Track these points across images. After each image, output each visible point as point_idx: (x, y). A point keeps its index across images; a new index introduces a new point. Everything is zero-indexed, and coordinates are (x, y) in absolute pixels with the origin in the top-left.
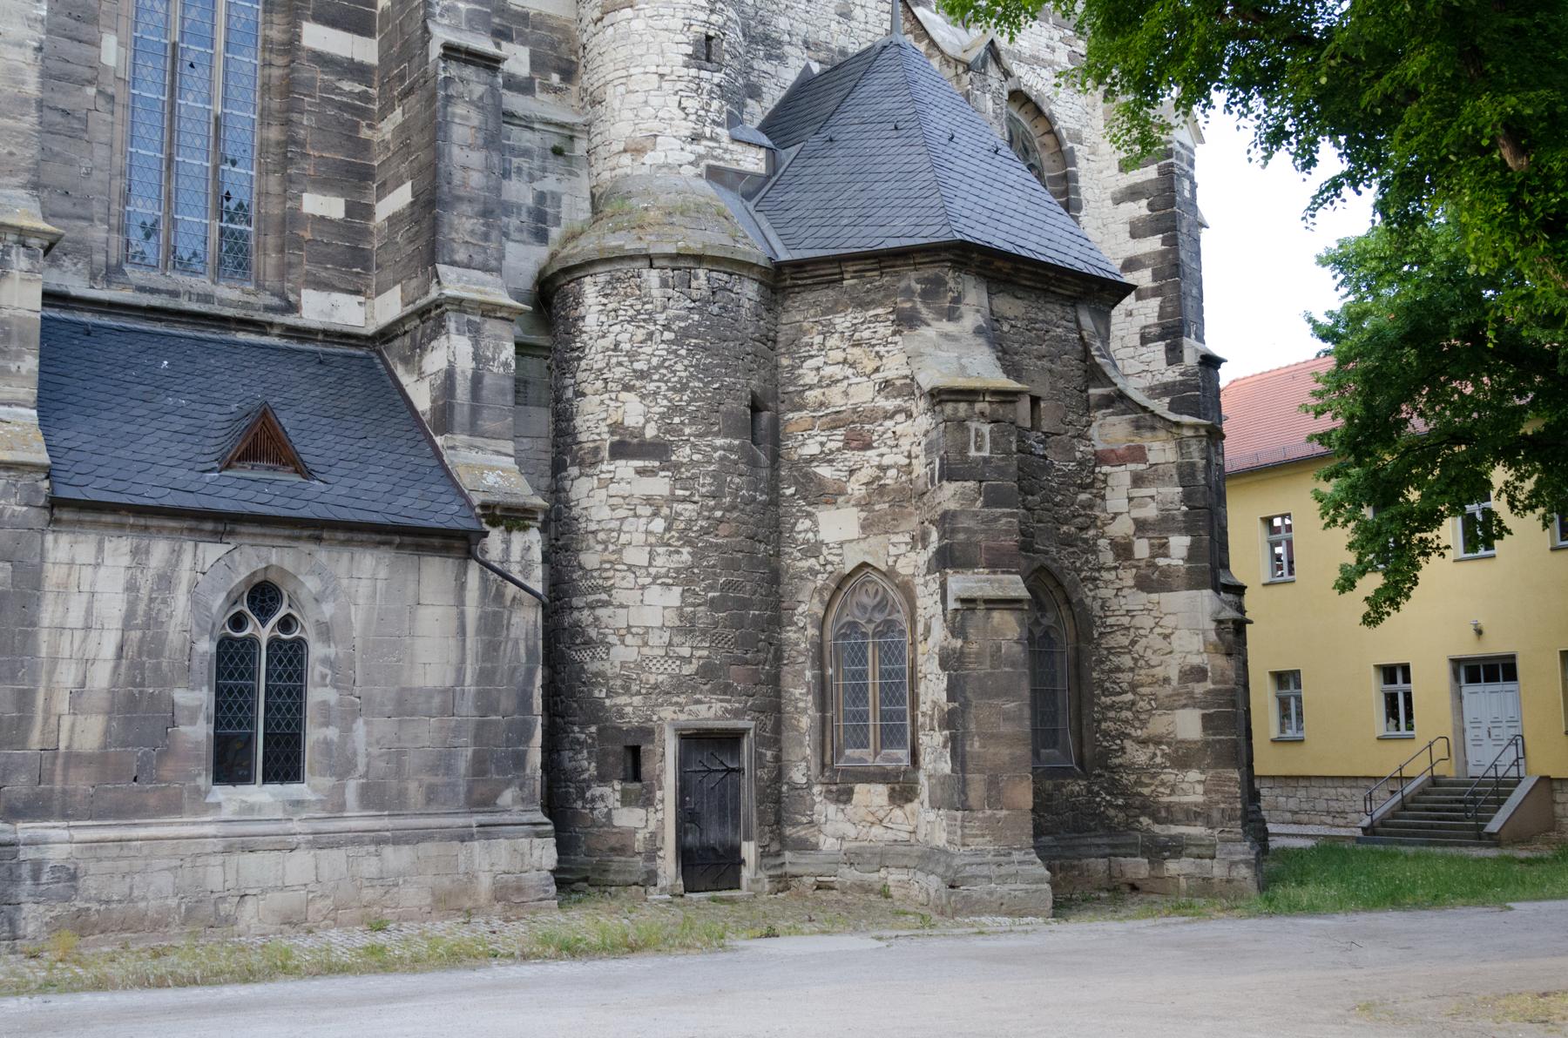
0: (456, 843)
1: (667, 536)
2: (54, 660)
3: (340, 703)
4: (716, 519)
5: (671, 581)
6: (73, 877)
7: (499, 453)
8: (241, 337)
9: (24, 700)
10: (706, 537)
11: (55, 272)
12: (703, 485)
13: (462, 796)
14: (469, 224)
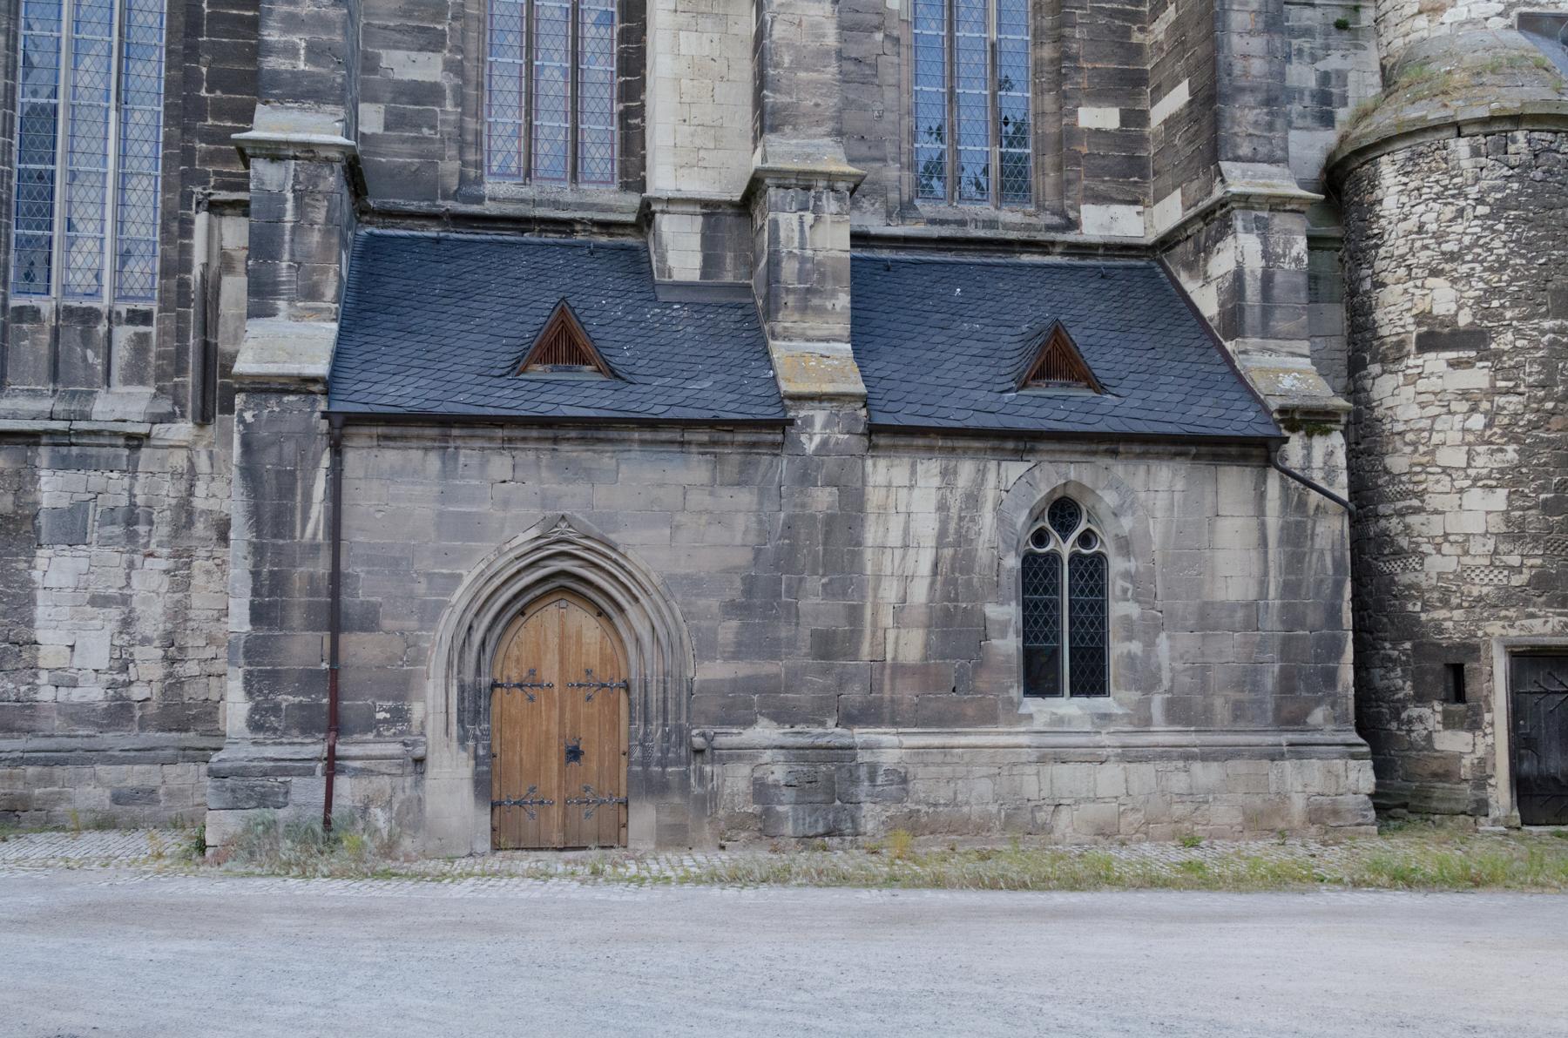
0: (1266, 763)
1: (1488, 433)
2: (878, 577)
3: (1143, 617)
4: (1546, 411)
5: (1494, 483)
6: (904, 780)
7: (1293, 354)
8: (1026, 258)
9: (855, 614)
10: (1535, 433)
11: (856, 213)
12: (1530, 374)
13: (1270, 714)
14: (1251, 115)
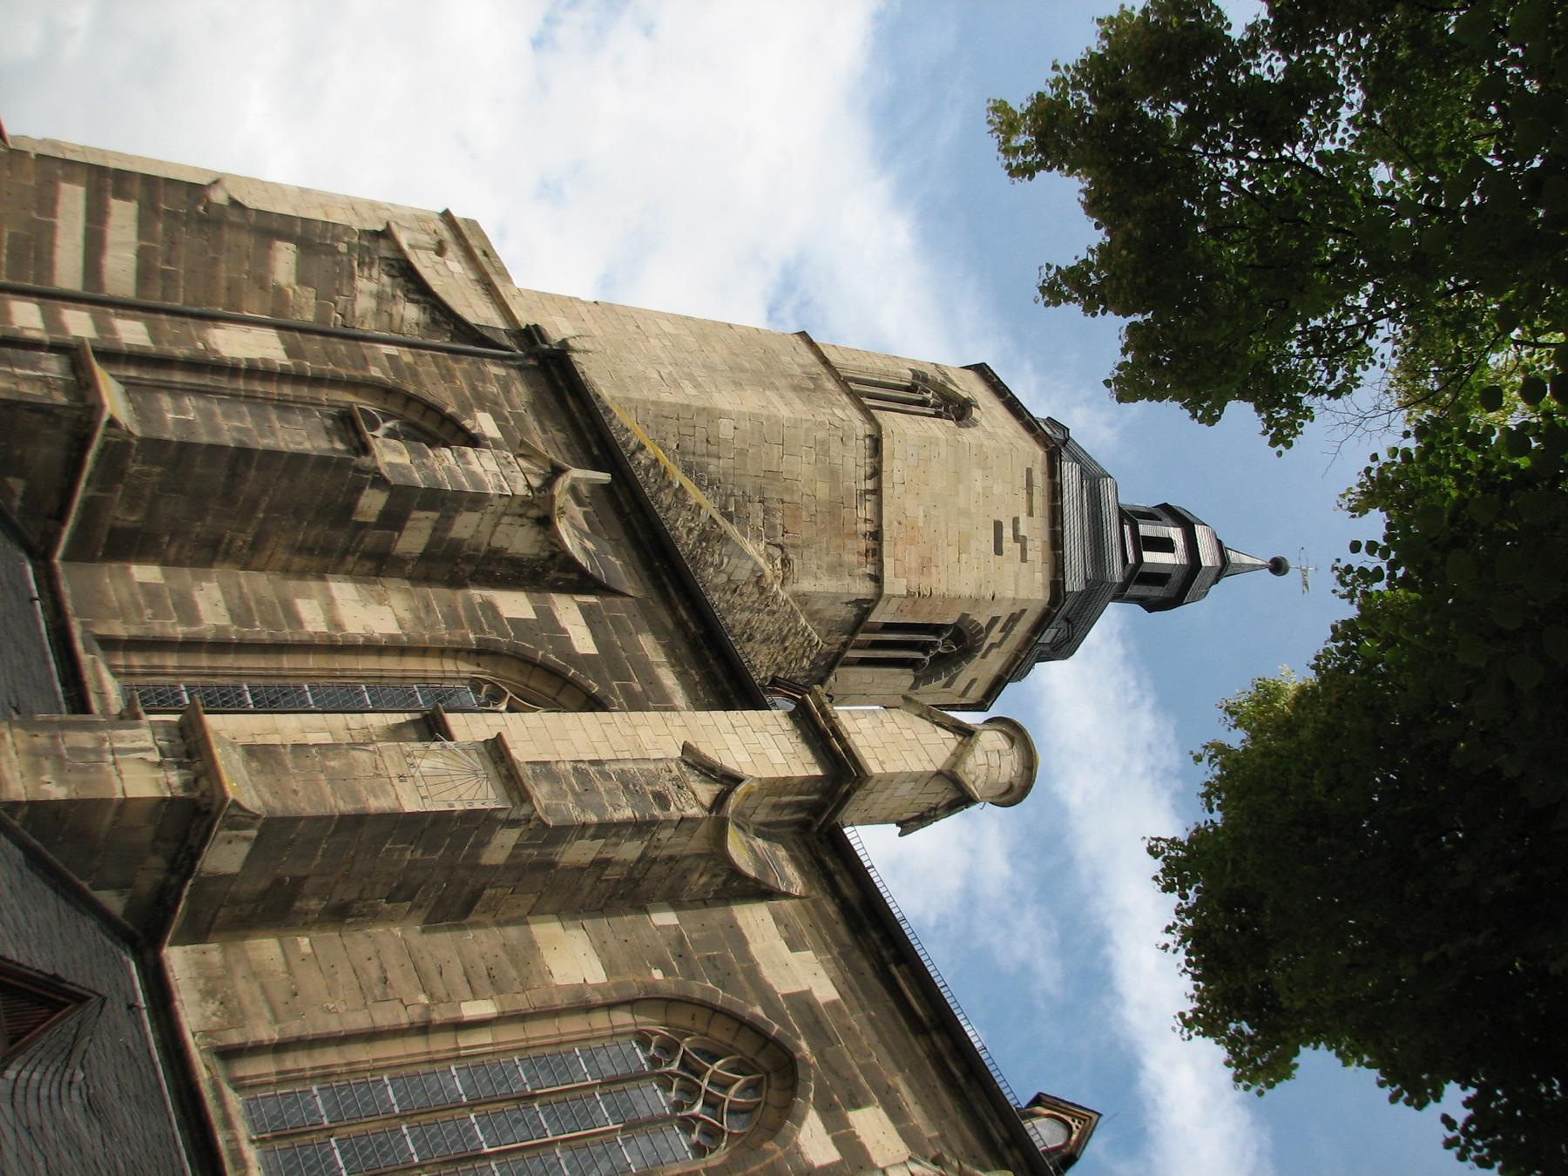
11: (196, 996)
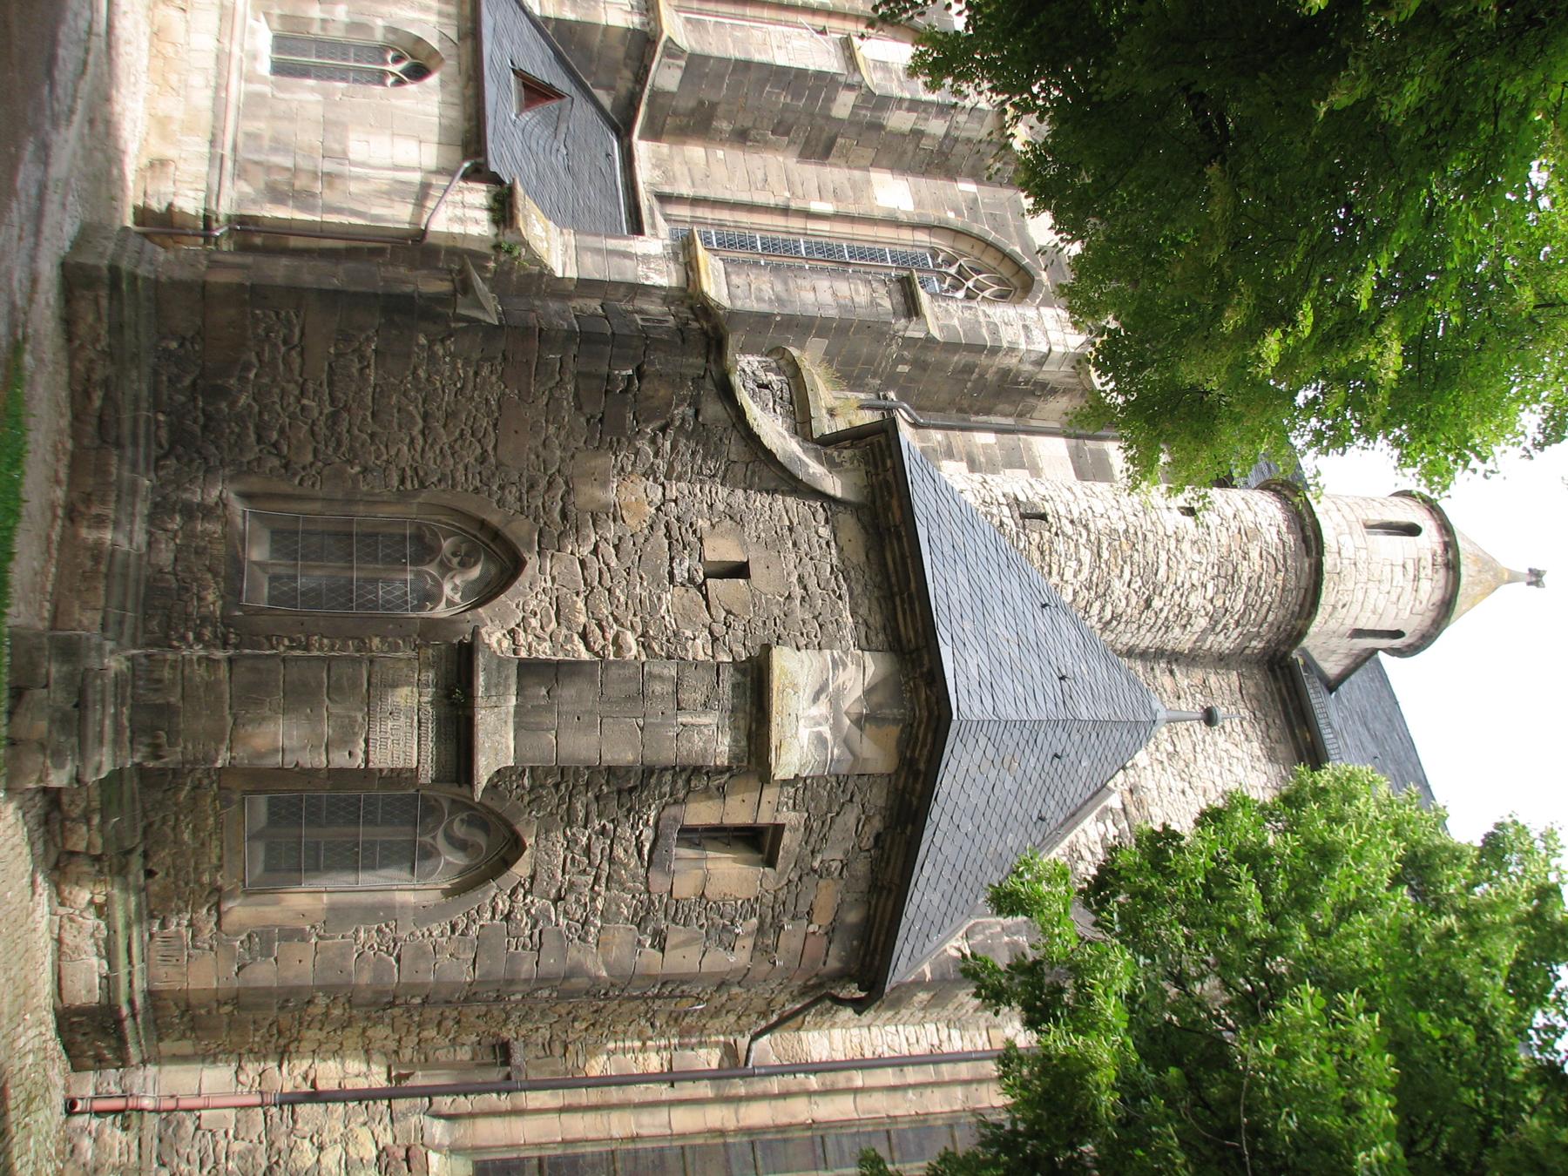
0: (209, 136)
14: (766, 287)
